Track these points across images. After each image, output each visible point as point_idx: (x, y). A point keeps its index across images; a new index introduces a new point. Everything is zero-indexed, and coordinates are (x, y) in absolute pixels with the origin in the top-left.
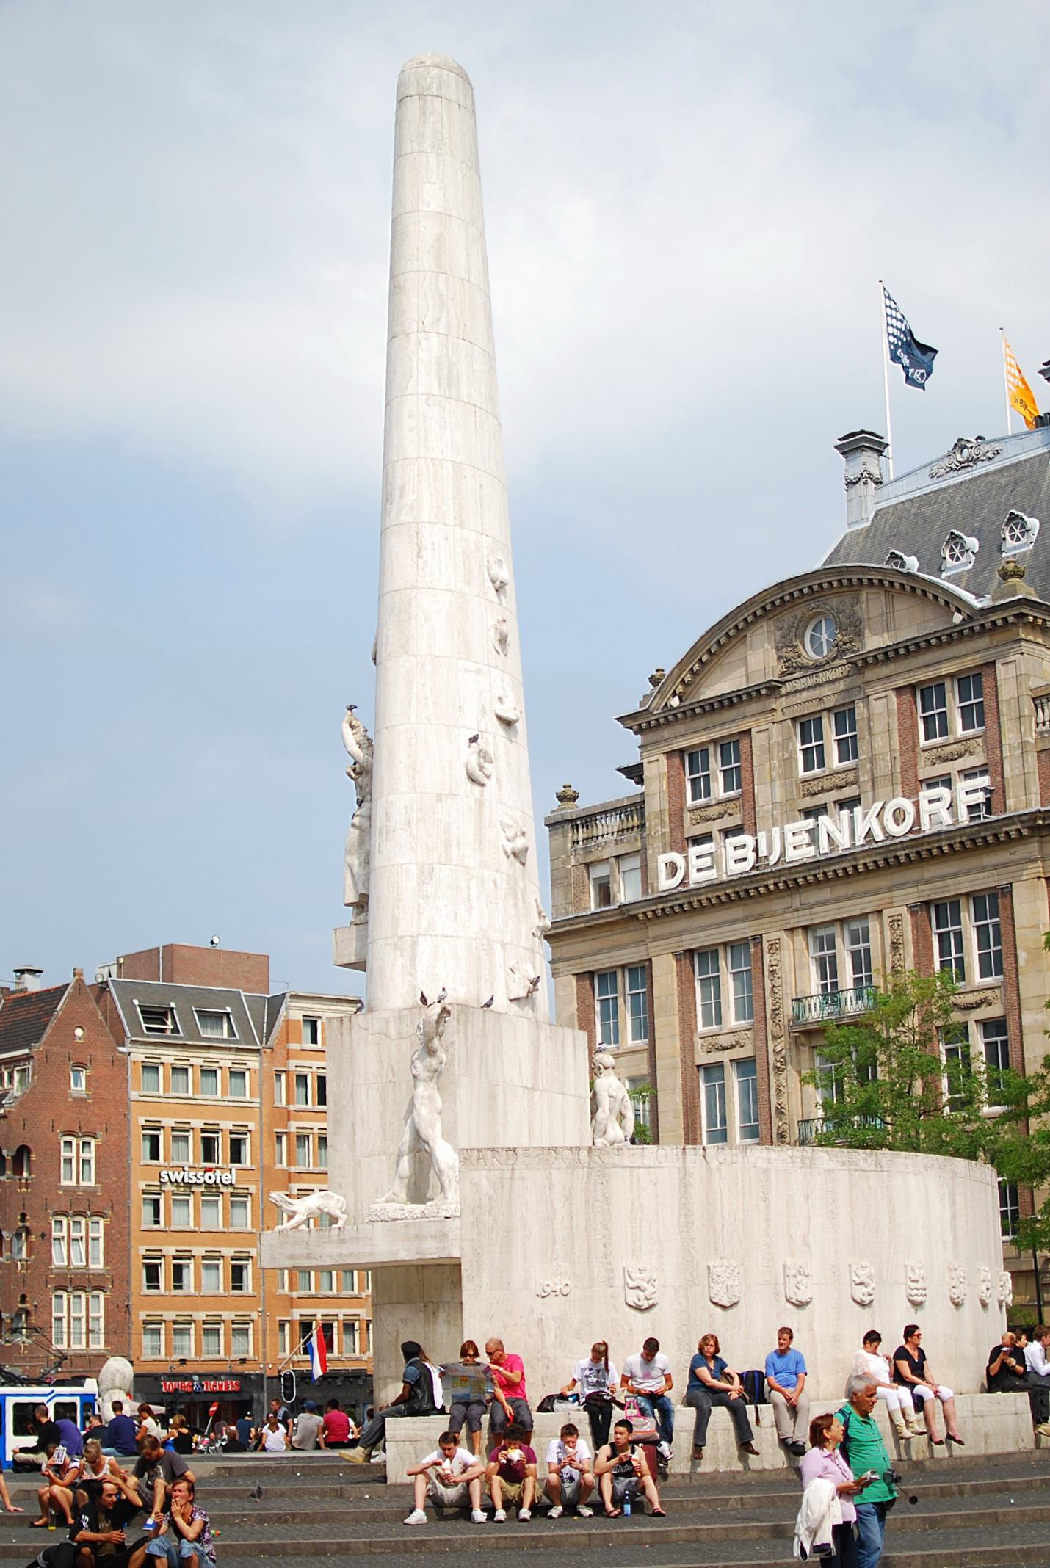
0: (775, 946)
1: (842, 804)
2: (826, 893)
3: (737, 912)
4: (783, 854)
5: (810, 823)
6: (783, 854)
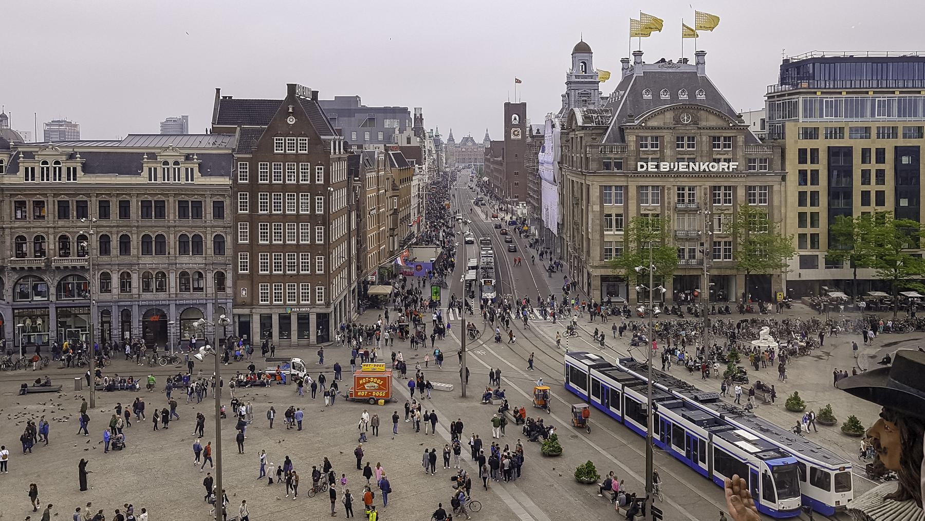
0: (669, 189)
3: (659, 179)
6: (678, 169)
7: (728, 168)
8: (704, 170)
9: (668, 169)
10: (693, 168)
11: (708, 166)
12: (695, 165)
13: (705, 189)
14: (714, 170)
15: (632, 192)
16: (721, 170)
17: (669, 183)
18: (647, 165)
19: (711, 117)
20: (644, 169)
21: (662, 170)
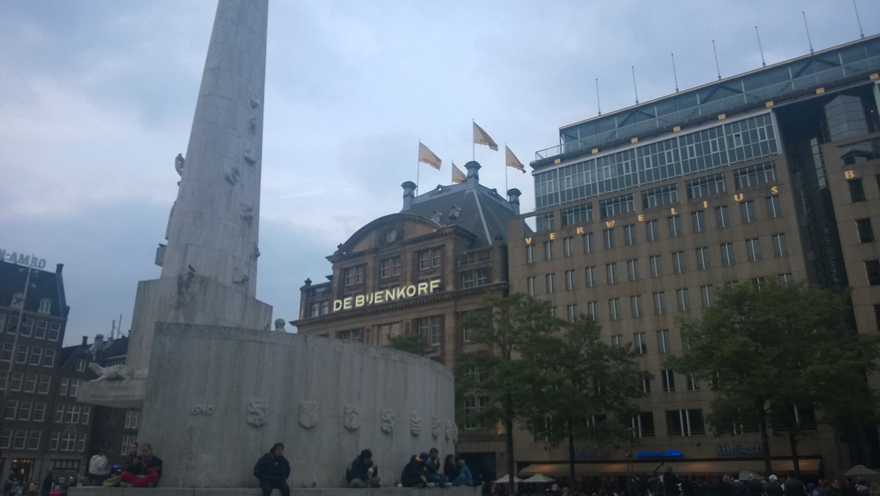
0: (368, 331)
2: (386, 315)
7: (428, 289)
8: (401, 297)
11: (405, 291)
13: (407, 324)
21: (357, 305)
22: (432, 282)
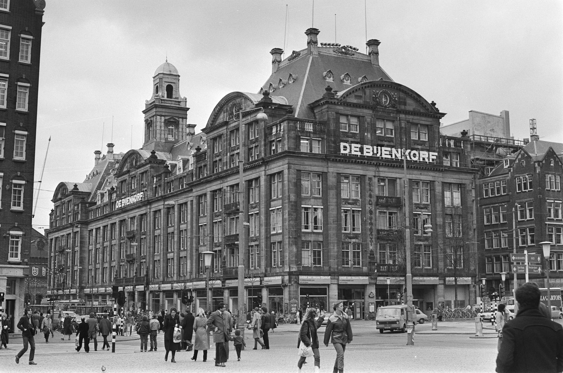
0: (370, 179)
1: (388, 146)
4: (381, 155)
5: (389, 149)
6: (381, 155)
7: (429, 158)
9: (371, 154)
10: (396, 156)
12: (398, 152)
14: (416, 159)
15: (332, 180)
16: (421, 160)
17: (370, 172)
18: (351, 147)
19: (409, 101)
20: (347, 152)
22: (431, 153)
